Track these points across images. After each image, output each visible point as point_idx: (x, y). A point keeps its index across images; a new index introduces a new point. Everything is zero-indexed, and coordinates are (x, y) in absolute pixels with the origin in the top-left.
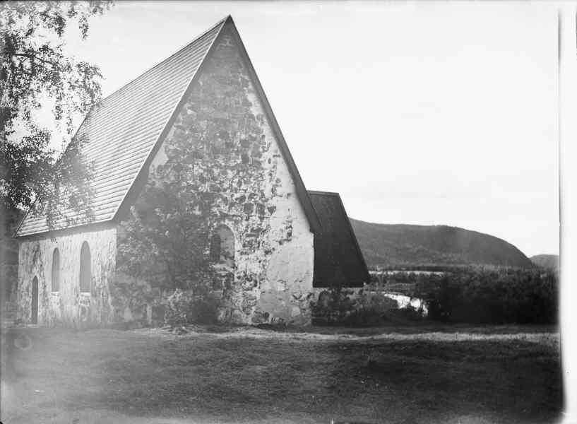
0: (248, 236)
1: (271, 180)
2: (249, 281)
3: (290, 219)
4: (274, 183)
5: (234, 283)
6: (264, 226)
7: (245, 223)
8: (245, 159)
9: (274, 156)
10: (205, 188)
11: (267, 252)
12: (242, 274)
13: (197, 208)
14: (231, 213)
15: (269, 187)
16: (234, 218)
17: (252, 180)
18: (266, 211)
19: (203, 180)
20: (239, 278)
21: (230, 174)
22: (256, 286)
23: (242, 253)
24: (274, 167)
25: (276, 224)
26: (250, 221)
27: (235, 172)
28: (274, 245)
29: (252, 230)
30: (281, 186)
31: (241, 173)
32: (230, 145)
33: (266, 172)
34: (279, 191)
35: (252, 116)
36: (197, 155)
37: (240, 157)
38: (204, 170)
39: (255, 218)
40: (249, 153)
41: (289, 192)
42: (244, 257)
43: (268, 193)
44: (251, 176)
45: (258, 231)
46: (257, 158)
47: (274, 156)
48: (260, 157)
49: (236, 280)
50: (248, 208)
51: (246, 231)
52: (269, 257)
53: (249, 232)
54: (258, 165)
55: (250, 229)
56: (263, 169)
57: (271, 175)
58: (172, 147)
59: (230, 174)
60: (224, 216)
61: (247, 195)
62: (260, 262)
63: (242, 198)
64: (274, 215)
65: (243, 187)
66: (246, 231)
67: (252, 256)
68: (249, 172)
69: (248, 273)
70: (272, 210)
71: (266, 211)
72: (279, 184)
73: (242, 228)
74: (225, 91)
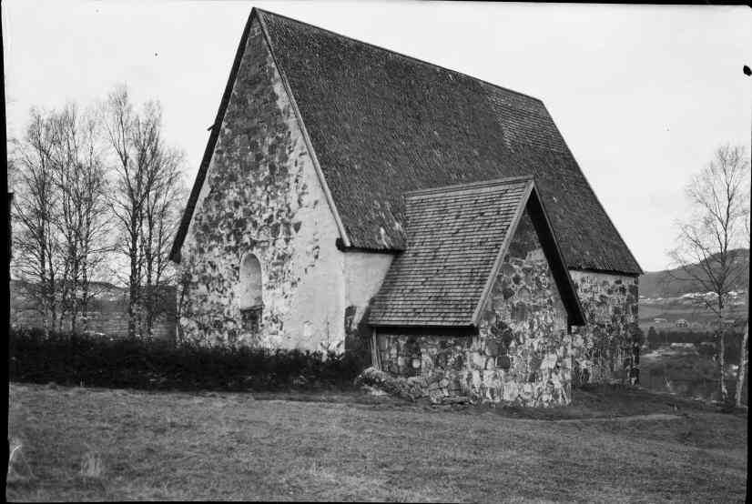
0: (275, 265)
1: (297, 188)
2: (275, 321)
3: (316, 237)
4: (300, 191)
5: (262, 326)
6: (290, 250)
7: (271, 249)
8: (272, 168)
9: (301, 154)
10: (239, 214)
11: (293, 284)
12: (269, 314)
13: (232, 237)
14: (260, 240)
15: (295, 198)
16: (262, 245)
17: (279, 194)
18: (292, 230)
19: (237, 205)
20: (266, 318)
21: (259, 191)
22: (281, 329)
23: (269, 288)
24: (301, 170)
25: (300, 242)
26: (276, 245)
27: (264, 188)
28: (297, 273)
29: (279, 258)
30: (307, 193)
31: (269, 189)
32: (259, 157)
33: (292, 180)
34: (306, 199)
35: (279, 113)
36: (232, 178)
37: (268, 167)
38: (238, 193)
39: (281, 242)
40: (277, 160)
41: (317, 198)
42: (271, 291)
43: (294, 205)
44: (278, 187)
45: (284, 258)
46: (284, 165)
47: (301, 154)
48: (286, 161)
49: (264, 322)
50: (275, 230)
51: (273, 259)
52: (295, 290)
53: (275, 260)
54: (285, 170)
55: (275, 258)
56: (289, 176)
57: (297, 181)
58: (214, 176)
59: (259, 191)
60: (254, 243)
61: (275, 214)
62: (286, 297)
63: (270, 219)
64: (299, 232)
65: (271, 205)
66: (273, 259)
67: (279, 291)
68: (276, 183)
69: (275, 312)
70: (297, 227)
71: (292, 230)
72: (306, 191)
73: (269, 256)
74: (254, 92)
